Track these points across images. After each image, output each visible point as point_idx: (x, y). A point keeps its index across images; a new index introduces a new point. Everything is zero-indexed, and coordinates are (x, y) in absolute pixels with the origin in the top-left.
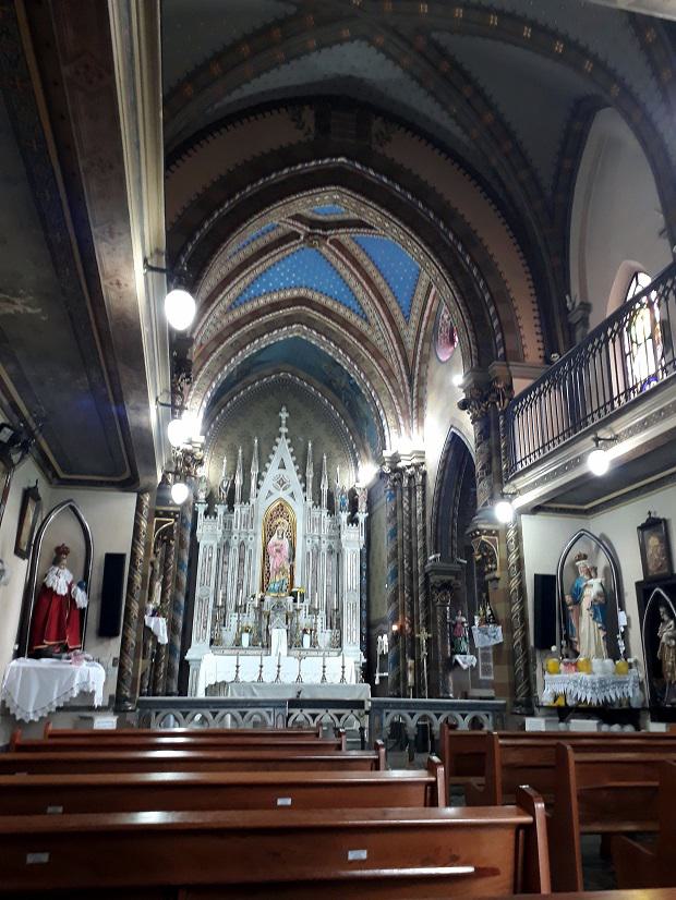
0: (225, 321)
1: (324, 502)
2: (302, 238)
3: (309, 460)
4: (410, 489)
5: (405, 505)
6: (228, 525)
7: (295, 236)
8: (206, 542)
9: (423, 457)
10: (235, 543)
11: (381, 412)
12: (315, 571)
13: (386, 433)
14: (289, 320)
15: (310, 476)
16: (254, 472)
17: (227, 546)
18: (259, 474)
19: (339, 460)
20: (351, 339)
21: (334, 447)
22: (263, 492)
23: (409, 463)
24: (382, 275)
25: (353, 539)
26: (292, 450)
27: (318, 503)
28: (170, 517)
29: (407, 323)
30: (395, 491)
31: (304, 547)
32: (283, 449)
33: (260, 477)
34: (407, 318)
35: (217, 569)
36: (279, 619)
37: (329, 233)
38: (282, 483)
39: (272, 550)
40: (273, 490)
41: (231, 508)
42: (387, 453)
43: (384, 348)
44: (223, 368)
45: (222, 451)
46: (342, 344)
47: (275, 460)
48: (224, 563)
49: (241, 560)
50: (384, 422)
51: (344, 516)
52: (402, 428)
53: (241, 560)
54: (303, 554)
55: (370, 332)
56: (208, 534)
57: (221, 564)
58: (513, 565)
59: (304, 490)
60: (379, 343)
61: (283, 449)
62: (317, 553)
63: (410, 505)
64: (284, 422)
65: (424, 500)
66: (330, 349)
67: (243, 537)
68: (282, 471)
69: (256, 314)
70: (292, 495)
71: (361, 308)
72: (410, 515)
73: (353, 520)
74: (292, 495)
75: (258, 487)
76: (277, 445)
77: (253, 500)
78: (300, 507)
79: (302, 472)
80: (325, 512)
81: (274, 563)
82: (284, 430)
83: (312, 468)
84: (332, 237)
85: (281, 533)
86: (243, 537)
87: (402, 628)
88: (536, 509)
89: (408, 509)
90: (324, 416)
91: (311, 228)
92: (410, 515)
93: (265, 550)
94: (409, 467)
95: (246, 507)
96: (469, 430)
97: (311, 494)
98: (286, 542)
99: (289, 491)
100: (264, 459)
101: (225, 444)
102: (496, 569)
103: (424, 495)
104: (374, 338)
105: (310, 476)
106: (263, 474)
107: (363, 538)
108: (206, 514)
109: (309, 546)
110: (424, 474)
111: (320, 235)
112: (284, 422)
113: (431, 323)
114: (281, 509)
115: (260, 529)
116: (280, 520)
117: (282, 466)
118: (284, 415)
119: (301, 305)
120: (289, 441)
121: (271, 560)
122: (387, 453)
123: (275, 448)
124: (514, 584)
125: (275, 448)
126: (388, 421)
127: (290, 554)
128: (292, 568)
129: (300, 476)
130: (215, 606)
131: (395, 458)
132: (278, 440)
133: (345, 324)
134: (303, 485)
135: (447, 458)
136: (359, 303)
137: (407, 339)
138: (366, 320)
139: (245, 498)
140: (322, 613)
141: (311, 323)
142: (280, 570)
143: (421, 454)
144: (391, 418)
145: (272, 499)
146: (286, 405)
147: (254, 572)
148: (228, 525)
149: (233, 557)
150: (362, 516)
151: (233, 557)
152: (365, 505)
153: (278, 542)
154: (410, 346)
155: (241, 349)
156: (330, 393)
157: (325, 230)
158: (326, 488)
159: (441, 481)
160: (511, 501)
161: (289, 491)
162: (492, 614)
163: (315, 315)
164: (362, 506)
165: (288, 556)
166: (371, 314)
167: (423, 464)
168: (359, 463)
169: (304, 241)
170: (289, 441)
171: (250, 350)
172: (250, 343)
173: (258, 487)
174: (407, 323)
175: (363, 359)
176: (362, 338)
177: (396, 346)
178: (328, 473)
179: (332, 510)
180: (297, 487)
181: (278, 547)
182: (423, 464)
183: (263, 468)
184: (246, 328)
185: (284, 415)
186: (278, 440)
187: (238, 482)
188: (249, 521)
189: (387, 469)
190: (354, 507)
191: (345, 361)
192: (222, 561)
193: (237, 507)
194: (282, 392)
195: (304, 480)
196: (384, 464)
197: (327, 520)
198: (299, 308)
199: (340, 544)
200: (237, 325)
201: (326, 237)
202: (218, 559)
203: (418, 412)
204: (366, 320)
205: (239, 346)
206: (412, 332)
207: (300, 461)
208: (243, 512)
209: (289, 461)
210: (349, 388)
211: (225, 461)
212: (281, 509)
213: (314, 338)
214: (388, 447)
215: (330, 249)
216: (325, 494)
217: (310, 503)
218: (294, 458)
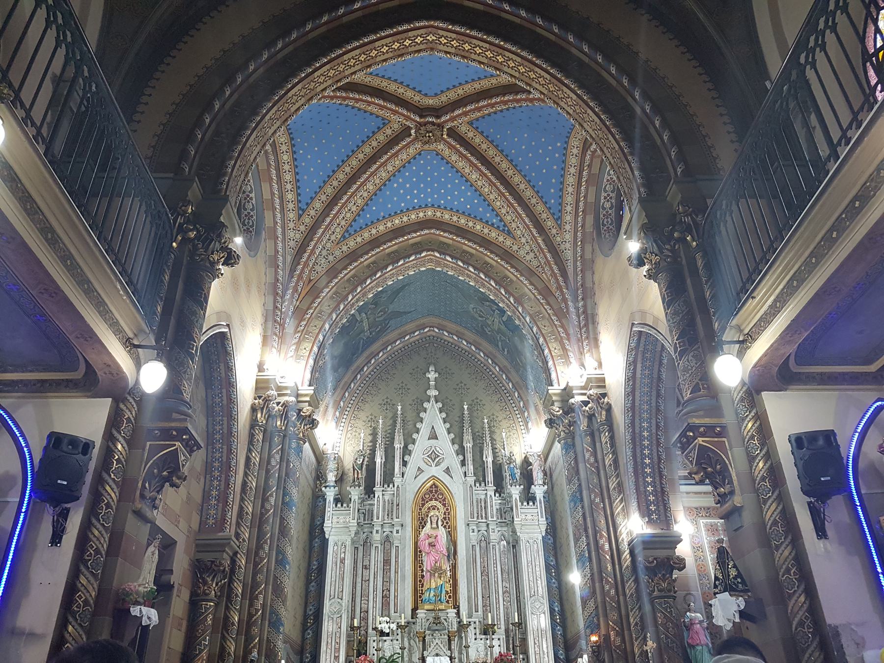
0: (338, 253)
1: (490, 477)
2: (413, 131)
3: (466, 425)
4: (592, 435)
5: (587, 455)
6: (366, 516)
7: (405, 132)
8: (336, 538)
9: (604, 387)
10: (377, 537)
11: (541, 340)
12: (485, 573)
13: (550, 363)
14: (417, 248)
15: (468, 445)
16: (398, 446)
17: (367, 544)
18: (406, 447)
19: (505, 424)
20: (492, 259)
21: (497, 407)
22: (411, 470)
23: (585, 398)
24: (520, 171)
25: (531, 524)
26: (444, 415)
27: (481, 479)
28: (173, 438)
29: (560, 226)
30: (573, 438)
31: (468, 539)
32: (433, 416)
33: (406, 451)
34: (558, 220)
35: (355, 576)
36: (438, 641)
37: (443, 119)
38: (434, 457)
39: (424, 545)
40: (424, 466)
41: (369, 491)
42: (555, 389)
43: (535, 263)
44: (338, 305)
45: (360, 423)
46: (484, 268)
47: (424, 429)
48: (366, 567)
49: (387, 562)
50: (546, 351)
51: (515, 492)
52: (570, 354)
53: (387, 562)
54: (467, 550)
55: (515, 248)
56: (338, 526)
57: (360, 572)
58: (763, 479)
59: (463, 463)
60: (528, 258)
61: (433, 416)
62: (485, 541)
63: (595, 454)
64: (432, 383)
65: (613, 444)
66: (470, 277)
67: (387, 530)
68: (433, 441)
69: (375, 242)
70: (447, 471)
71: (501, 220)
72: (598, 468)
73: (529, 497)
74: (447, 471)
75: (405, 464)
76: (425, 410)
77: (397, 480)
78: (458, 486)
79: (458, 441)
80: (491, 488)
81: (428, 562)
82: (433, 393)
83: (472, 438)
84: (450, 125)
85: (434, 520)
86: (387, 530)
87: (607, 637)
88: (778, 374)
89: (592, 460)
90: (481, 372)
91: (421, 117)
92: (598, 468)
93: (416, 544)
94: (586, 403)
95: (390, 490)
96: (652, 297)
97: (471, 467)
98: (442, 532)
99: (444, 466)
100: (410, 426)
101: (363, 415)
102: (732, 493)
103: (612, 438)
104: (522, 253)
105: (468, 445)
106: (410, 447)
107: (543, 521)
108: (337, 501)
109: (474, 536)
110: (609, 409)
111: (433, 124)
112: (432, 383)
113: (590, 220)
114: (434, 492)
115: (408, 518)
116: (433, 503)
117: (434, 436)
118: (432, 375)
119: (430, 228)
120: (440, 405)
121: (425, 559)
122: (555, 389)
123: (422, 415)
124: (771, 511)
125: (422, 415)
126: (552, 349)
127: (448, 550)
128: (454, 568)
129: (456, 447)
130: (352, 628)
131: (567, 393)
132: (425, 405)
133: (485, 242)
134: (461, 457)
135: (634, 373)
136: (497, 215)
137: (562, 247)
138: (509, 233)
139: (388, 479)
140: (501, 633)
141: (444, 249)
142: (437, 571)
143: (601, 382)
144: (554, 345)
145: (423, 478)
146: (435, 365)
147: (403, 577)
148: (366, 516)
149: (376, 558)
150: (539, 490)
151: (376, 558)
152: (541, 475)
153: (434, 533)
154: (569, 254)
155: (360, 284)
156: (485, 344)
157: (438, 117)
158: (490, 459)
159: (632, 409)
160: (741, 354)
161: (444, 466)
162: (739, 575)
163: (446, 237)
164: (538, 476)
165: (445, 552)
166: (514, 225)
167: (604, 395)
168: (530, 424)
169: (416, 138)
170: (440, 405)
171: (372, 288)
172: (370, 276)
173: (405, 464)
174: (560, 226)
175: (511, 281)
176: (507, 256)
177: (548, 255)
178: (492, 439)
179: (500, 488)
180: (452, 459)
181: (431, 540)
182: (604, 395)
183: (409, 441)
184: (366, 259)
185: (432, 375)
186: (425, 405)
187: (379, 460)
188: (393, 508)
189: (556, 409)
190: (527, 478)
191: (489, 288)
192: (360, 566)
193: (378, 490)
194: (429, 350)
195: (461, 451)
196: (553, 404)
197: (495, 502)
198: (427, 231)
199: (514, 532)
200: (353, 256)
201: (441, 126)
202: (355, 562)
203: (587, 331)
204: (509, 233)
205: (358, 280)
206: (568, 237)
207: (456, 429)
208: (387, 498)
209: (441, 429)
210: (503, 327)
211: (362, 435)
212: (434, 492)
213: (450, 267)
214: (555, 382)
215: (451, 147)
216: (490, 465)
217: (471, 480)
218: (448, 425)
